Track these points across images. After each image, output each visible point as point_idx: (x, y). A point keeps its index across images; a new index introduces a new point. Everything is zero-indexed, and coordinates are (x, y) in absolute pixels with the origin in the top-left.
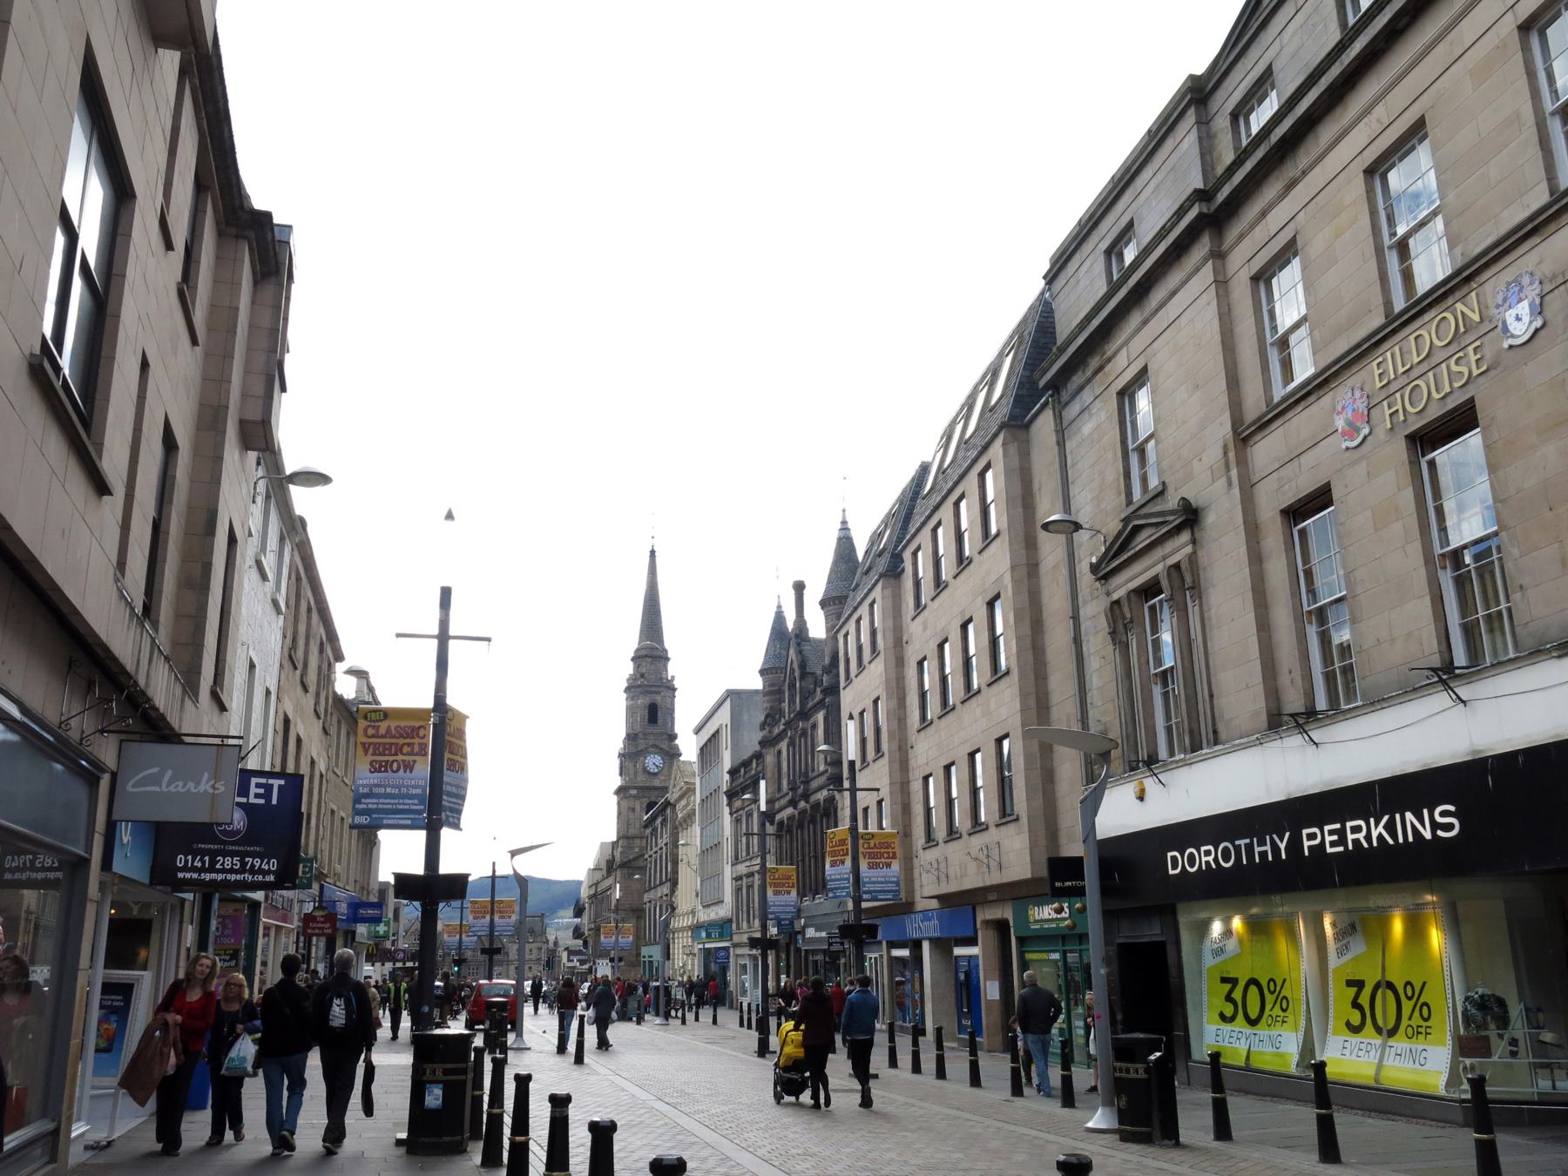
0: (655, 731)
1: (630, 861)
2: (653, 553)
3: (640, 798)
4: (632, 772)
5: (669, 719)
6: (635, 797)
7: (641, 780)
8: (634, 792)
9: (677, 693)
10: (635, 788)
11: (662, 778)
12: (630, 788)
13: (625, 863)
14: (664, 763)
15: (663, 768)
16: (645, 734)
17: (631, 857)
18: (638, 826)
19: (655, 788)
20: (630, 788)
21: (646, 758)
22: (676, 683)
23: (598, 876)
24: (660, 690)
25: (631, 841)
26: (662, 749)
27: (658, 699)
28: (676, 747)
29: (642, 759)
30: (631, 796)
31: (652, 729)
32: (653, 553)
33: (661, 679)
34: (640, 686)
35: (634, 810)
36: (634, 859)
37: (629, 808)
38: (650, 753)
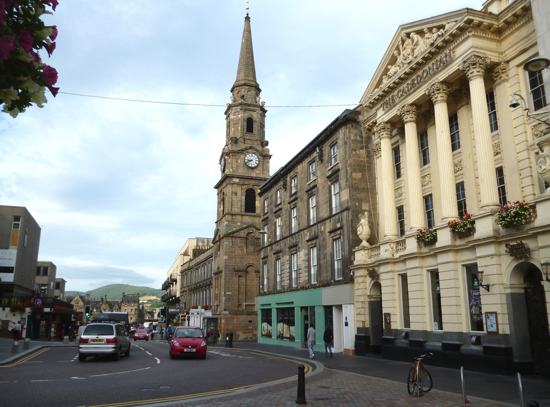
0: (251, 138)
1: (233, 232)
2: (247, 18)
7: (242, 172)
9: (266, 114)
10: (238, 177)
11: (258, 172)
17: (234, 229)
19: (252, 179)
21: (245, 156)
23: (187, 259)
24: (255, 108)
26: (257, 151)
29: (242, 156)
31: (248, 136)
32: (247, 18)
33: (256, 102)
34: (241, 104)
35: (236, 194)
36: (237, 231)
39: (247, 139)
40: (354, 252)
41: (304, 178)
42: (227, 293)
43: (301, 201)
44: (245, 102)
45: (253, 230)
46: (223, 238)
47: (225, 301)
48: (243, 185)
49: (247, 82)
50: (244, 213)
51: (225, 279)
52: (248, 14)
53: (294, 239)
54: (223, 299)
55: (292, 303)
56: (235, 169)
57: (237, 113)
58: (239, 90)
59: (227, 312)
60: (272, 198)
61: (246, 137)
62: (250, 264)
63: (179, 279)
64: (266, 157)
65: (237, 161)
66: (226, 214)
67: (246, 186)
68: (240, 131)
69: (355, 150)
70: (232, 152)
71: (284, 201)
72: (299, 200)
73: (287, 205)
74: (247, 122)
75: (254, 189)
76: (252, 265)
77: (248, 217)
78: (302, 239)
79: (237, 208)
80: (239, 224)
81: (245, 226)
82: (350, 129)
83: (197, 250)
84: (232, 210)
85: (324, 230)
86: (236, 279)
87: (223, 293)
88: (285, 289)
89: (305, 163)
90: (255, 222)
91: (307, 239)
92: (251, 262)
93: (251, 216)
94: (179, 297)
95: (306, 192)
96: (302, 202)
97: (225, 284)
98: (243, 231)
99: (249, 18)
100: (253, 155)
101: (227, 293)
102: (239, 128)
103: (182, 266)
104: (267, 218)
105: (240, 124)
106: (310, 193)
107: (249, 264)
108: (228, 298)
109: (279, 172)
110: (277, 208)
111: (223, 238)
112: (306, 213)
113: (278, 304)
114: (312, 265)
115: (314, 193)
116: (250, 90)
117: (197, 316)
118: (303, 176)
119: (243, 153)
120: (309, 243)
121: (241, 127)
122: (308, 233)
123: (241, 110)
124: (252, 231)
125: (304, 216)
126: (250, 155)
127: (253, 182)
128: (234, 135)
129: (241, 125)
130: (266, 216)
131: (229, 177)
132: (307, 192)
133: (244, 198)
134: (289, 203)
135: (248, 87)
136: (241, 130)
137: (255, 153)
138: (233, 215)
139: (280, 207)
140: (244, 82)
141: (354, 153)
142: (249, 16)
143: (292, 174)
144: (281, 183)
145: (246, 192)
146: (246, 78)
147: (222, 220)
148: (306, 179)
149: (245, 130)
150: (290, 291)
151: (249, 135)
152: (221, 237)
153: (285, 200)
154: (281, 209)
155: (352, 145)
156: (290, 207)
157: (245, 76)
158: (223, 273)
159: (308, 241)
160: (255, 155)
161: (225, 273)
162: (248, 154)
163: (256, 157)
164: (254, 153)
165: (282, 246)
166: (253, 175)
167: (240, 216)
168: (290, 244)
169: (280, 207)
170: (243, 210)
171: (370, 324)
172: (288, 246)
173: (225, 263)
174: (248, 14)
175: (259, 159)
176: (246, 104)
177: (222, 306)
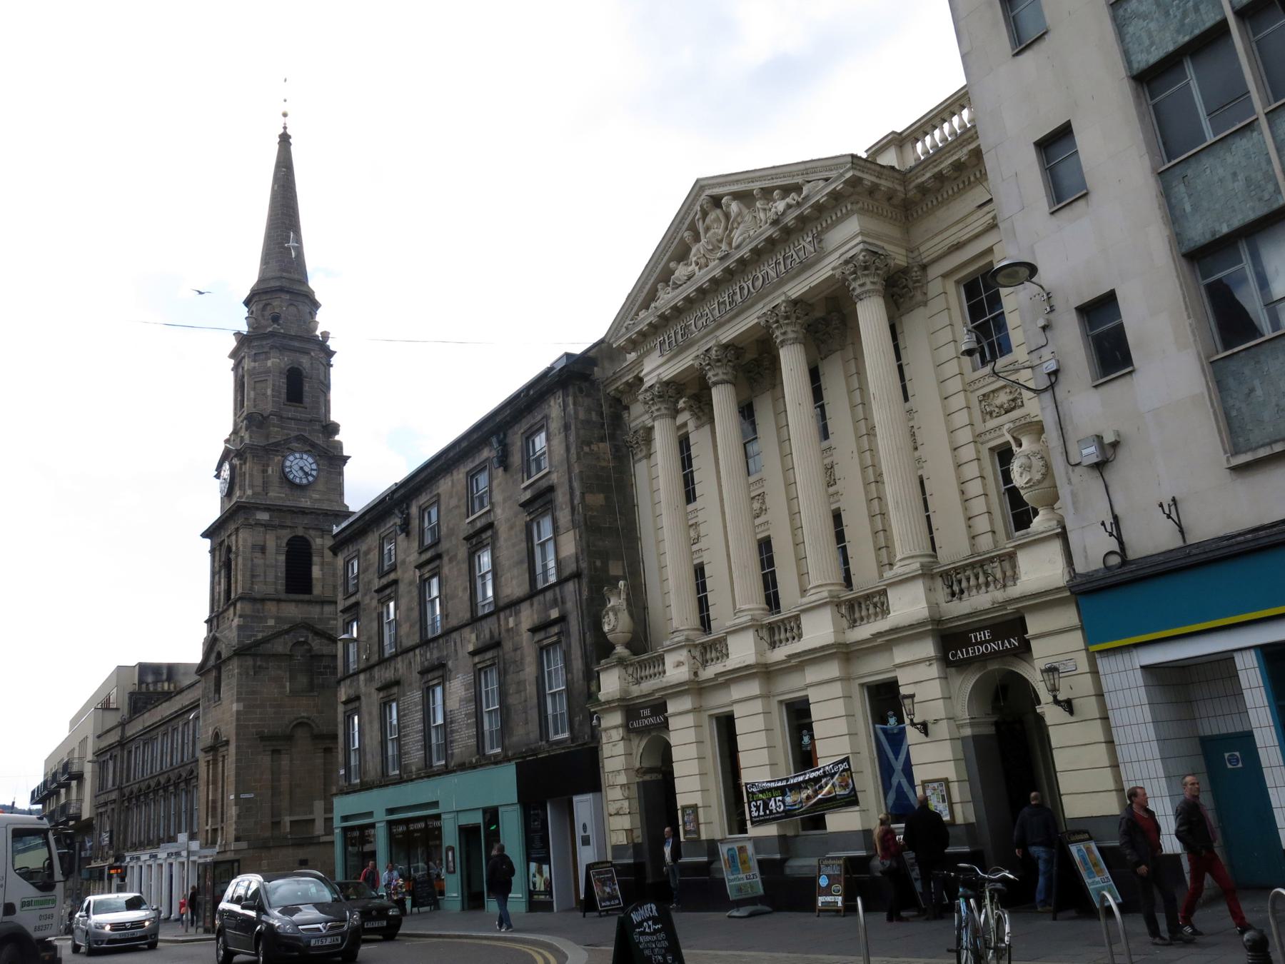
0: (298, 416)
1: (258, 643)
2: (285, 139)
3: (274, 527)
4: (258, 481)
5: (322, 399)
6: (267, 526)
7: (277, 495)
8: (263, 516)
9: (333, 360)
10: (267, 508)
11: (316, 496)
12: (258, 507)
13: (249, 647)
14: (318, 470)
15: (316, 478)
16: (281, 418)
17: (260, 636)
18: (271, 578)
19: (303, 512)
20: (258, 507)
21: (285, 458)
22: (332, 344)
23: (112, 719)
24: (307, 346)
25: (259, 606)
26: (313, 445)
27: (305, 361)
28: (339, 445)
29: (278, 459)
30: (259, 524)
31: (291, 412)
32: (285, 139)
35: (263, 549)
36: (266, 640)
37: (254, 547)
38: (293, 451)
39: (289, 418)
40: (598, 673)
41: (457, 507)
42: (242, 796)
43: (451, 560)
44: (282, 331)
45: (307, 637)
46: (229, 658)
47: (239, 816)
48: (283, 527)
49: (285, 284)
50: (283, 596)
51: (238, 761)
52: (285, 128)
53: (435, 652)
54: (233, 811)
55: (435, 804)
56: (259, 489)
57: (262, 357)
58: (266, 302)
59: (243, 845)
60: (369, 556)
61: (285, 414)
62: (300, 720)
63: (88, 770)
64: (334, 460)
65: (265, 471)
66: (241, 599)
67: (288, 531)
68: (270, 399)
69: (589, 444)
70: (252, 449)
71: (403, 562)
72: (446, 559)
73: (412, 573)
74: (288, 378)
75: (307, 536)
76: (305, 720)
77: (293, 604)
78: (456, 650)
79: (265, 583)
80: (271, 622)
81: (286, 627)
82: (575, 398)
83: (140, 693)
84: (251, 589)
85: (516, 625)
86: (266, 760)
87: (232, 797)
88: (411, 772)
89: (460, 475)
90: (312, 616)
91: (471, 648)
92: (303, 714)
93: (302, 601)
94: (90, 820)
95: (464, 539)
96: (454, 563)
97: (237, 775)
98: (282, 640)
99: (290, 137)
100: (305, 456)
101: (242, 796)
102: (269, 392)
103: (99, 737)
104: (357, 604)
105: (270, 383)
106: (474, 541)
107: (297, 719)
108: (245, 809)
109: (388, 495)
110: (384, 581)
111: (229, 658)
112: (465, 589)
113: (391, 811)
114: (485, 709)
115: (485, 542)
116: (295, 303)
117: (148, 863)
118: (454, 502)
119: (278, 451)
120: (477, 659)
121: (273, 390)
122: (473, 637)
123: (271, 348)
124: (302, 639)
125: (460, 594)
126: (297, 455)
127: (306, 520)
128: (255, 407)
129: (274, 385)
130: (353, 600)
131: (244, 508)
132: (467, 539)
133: (282, 558)
134: (419, 567)
135: (288, 297)
136: (273, 396)
137: (309, 451)
138: (254, 600)
139: (392, 576)
140: (278, 284)
141: (586, 449)
142: (289, 132)
143: (424, 499)
144: (396, 520)
145: (287, 544)
146: (284, 274)
147: (226, 615)
148: (464, 510)
149: (284, 396)
150: (429, 777)
151: (293, 408)
152: (224, 656)
153: (408, 559)
154: (395, 582)
155: (582, 432)
156: (420, 577)
157: (283, 270)
158: (232, 748)
159: (473, 654)
160: (309, 455)
161: (238, 747)
162: (291, 454)
163: (311, 460)
164: (306, 452)
165: (401, 671)
166: (305, 503)
167: (275, 603)
168: (422, 663)
169: (392, 576)
170: (281, 586)
171: (643, 835)
172: (417, 667)
173: (238, 719)
174: (285, 128)
175: (318, 465)
176: (284, 336)
177: (231, 831)
